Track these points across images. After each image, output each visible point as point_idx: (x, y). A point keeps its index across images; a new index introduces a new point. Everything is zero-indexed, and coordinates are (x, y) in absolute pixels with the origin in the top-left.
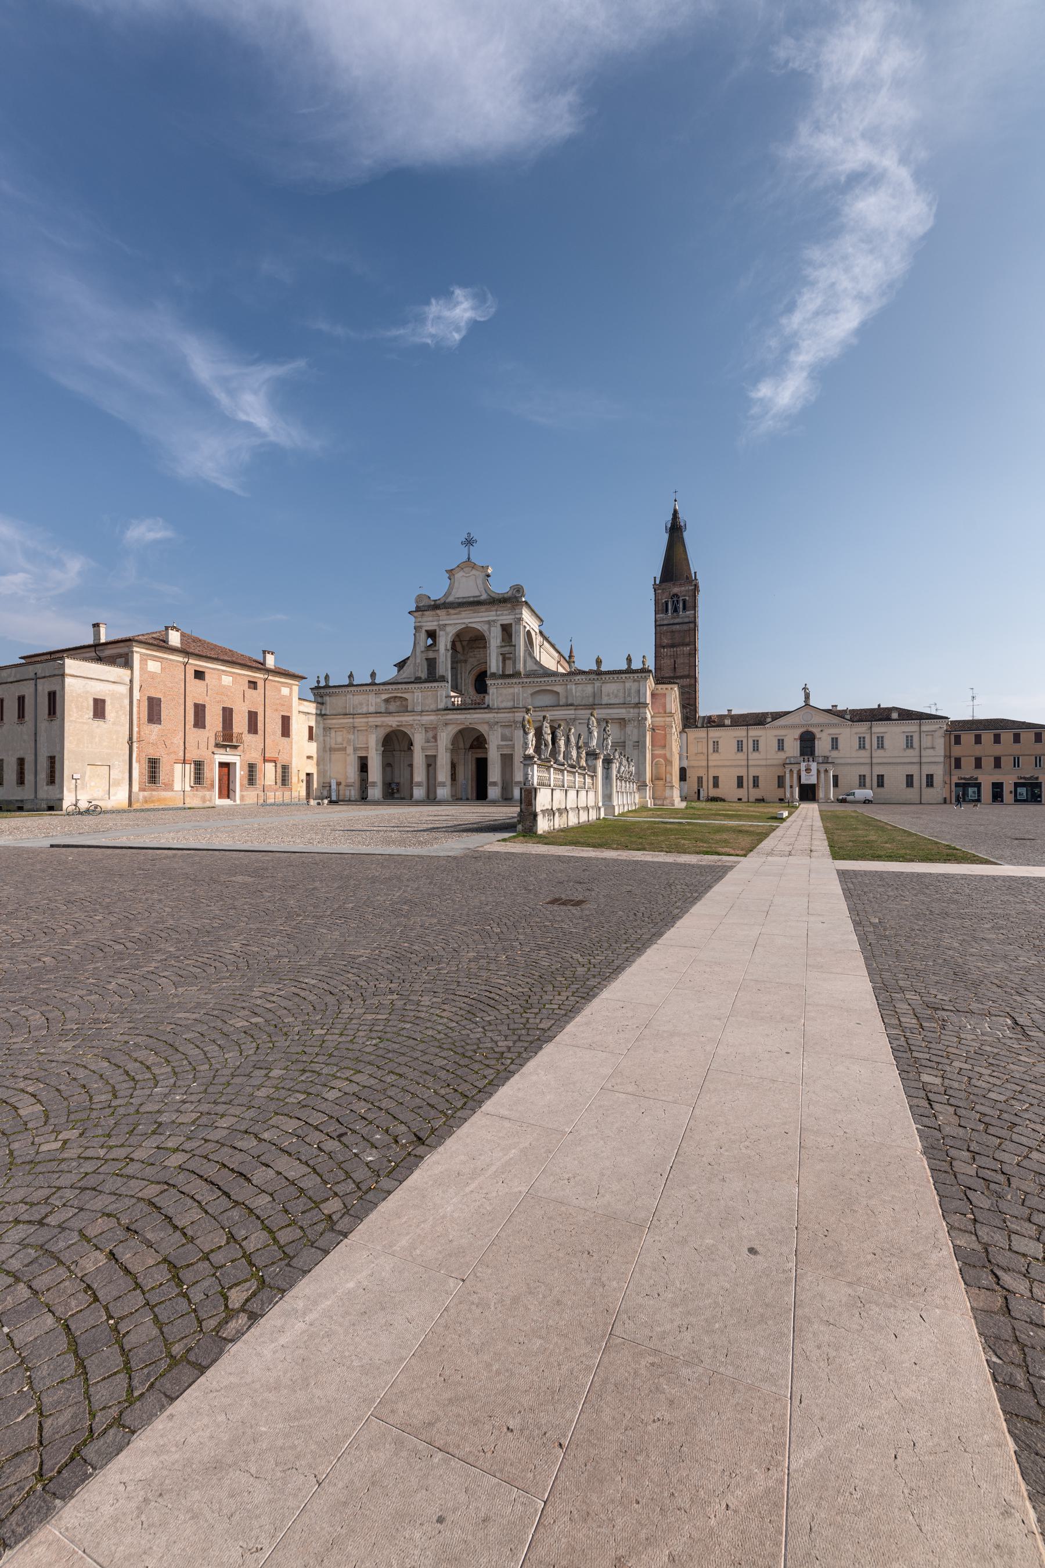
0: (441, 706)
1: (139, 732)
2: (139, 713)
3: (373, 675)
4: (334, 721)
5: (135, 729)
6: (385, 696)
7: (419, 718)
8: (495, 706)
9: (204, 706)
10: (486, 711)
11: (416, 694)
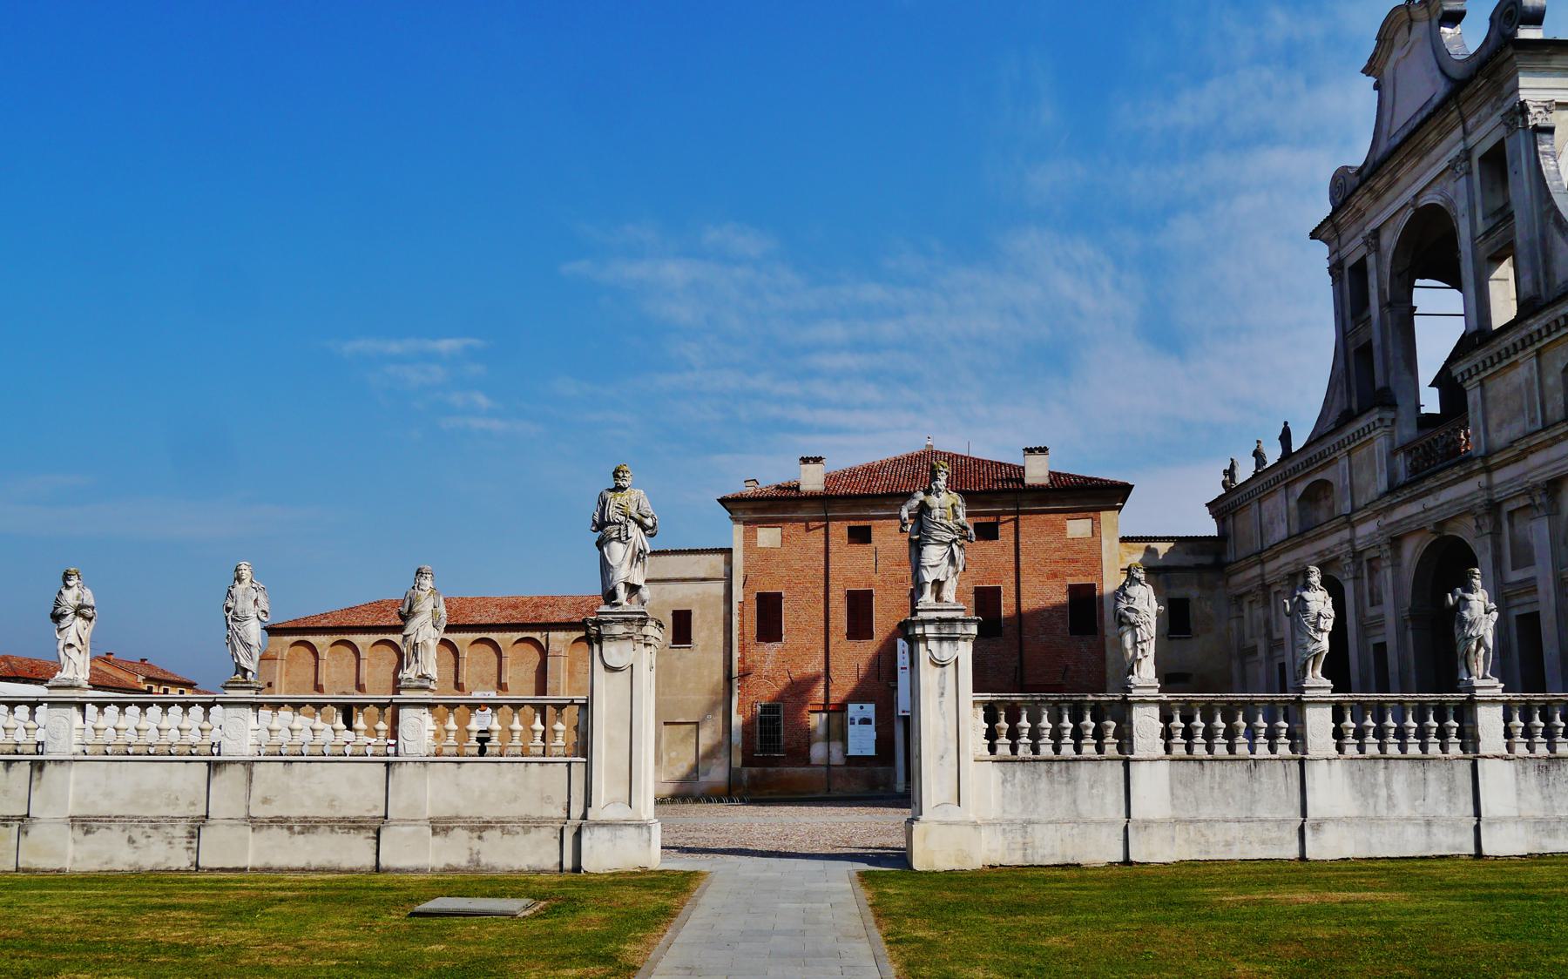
0: (1383, 485)
1: (742, 660)
2: (742, 625)
3: (1286, 437)
4: (1241, 577)
5: (736, 655)
6: (1300, 488)
7: (1346, 534)
8: (1482, 452)
9: (869, 594)
10: (1458, 471)
11: (1342, 463)
